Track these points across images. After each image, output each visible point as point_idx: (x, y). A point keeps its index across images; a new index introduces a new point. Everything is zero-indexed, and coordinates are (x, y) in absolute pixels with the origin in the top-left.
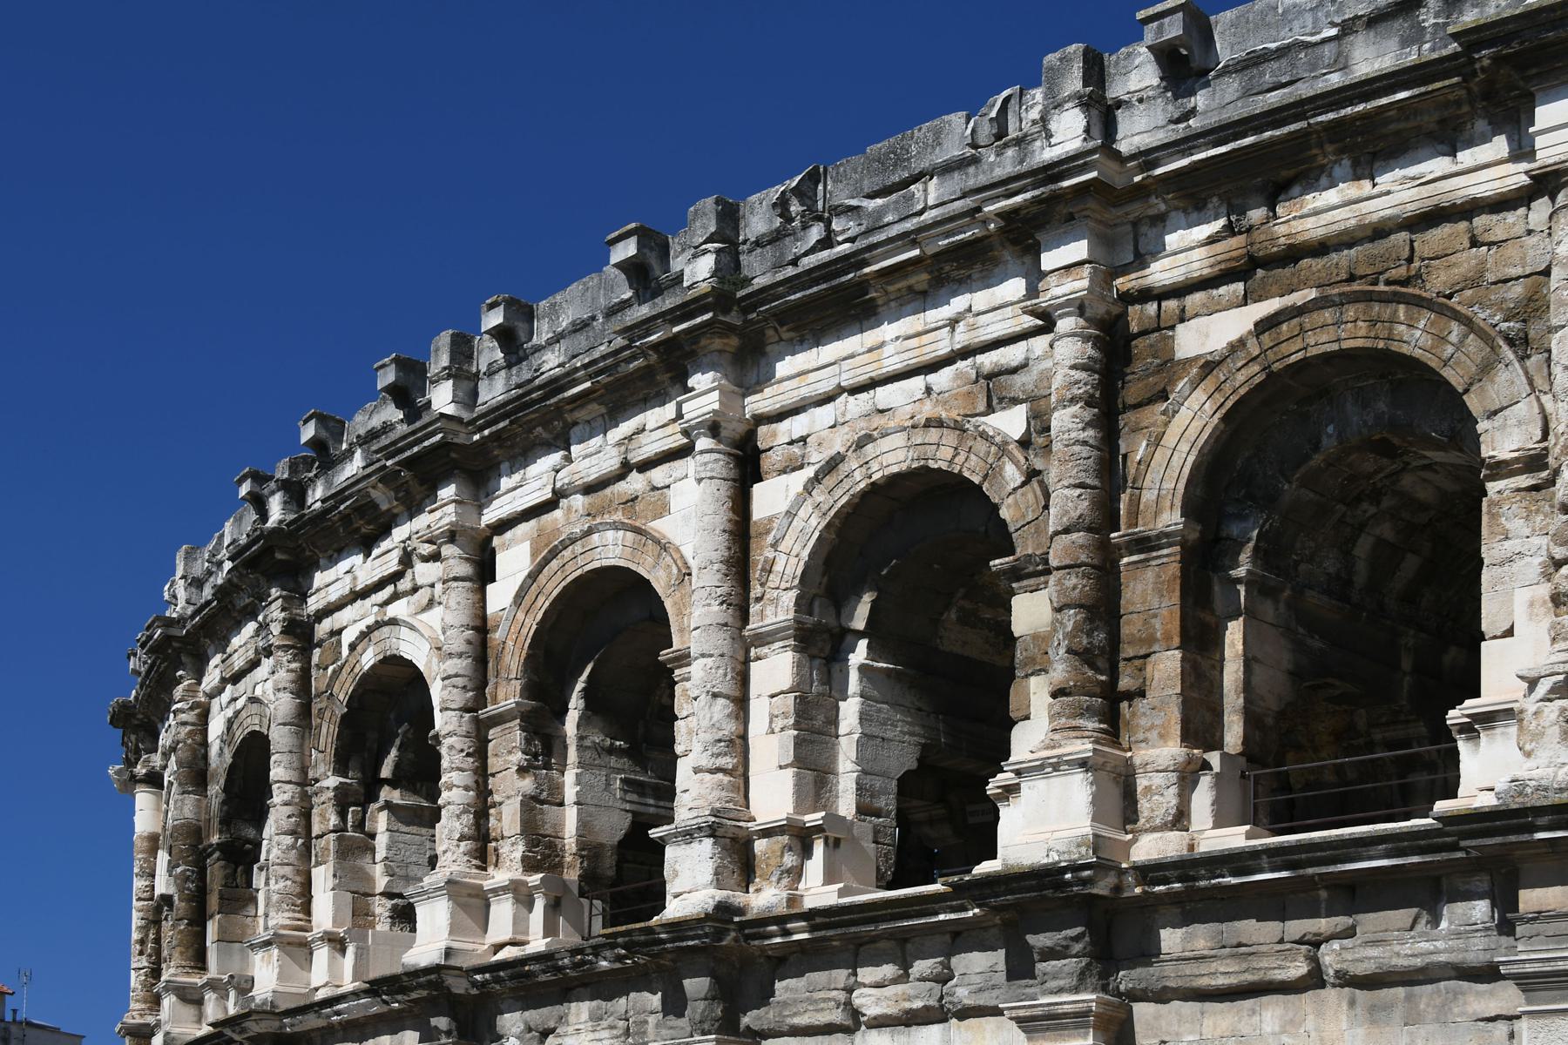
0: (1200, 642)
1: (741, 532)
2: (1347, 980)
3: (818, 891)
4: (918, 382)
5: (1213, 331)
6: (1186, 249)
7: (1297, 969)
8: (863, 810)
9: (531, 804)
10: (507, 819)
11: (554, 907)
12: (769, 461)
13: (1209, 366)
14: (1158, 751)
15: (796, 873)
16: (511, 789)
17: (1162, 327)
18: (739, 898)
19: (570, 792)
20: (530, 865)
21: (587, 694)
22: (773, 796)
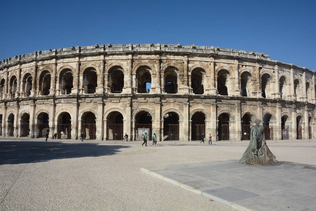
0: (40, 84)
1: (20, 75)
3: (23, 97)
4: (29, 68)
6: (40, 63)
7: (42, 103)
8: (26, 92)
9: (10, 90)
10: (9, 90)
11: (11, 96)
12: (22, 71)
14: (38, 91)
15: (22, 96)
16: (9, 88)
18: (19, 97)
19: (13, 88)
20: (10, 93)
21: (14, 82)
22: (21, 91)
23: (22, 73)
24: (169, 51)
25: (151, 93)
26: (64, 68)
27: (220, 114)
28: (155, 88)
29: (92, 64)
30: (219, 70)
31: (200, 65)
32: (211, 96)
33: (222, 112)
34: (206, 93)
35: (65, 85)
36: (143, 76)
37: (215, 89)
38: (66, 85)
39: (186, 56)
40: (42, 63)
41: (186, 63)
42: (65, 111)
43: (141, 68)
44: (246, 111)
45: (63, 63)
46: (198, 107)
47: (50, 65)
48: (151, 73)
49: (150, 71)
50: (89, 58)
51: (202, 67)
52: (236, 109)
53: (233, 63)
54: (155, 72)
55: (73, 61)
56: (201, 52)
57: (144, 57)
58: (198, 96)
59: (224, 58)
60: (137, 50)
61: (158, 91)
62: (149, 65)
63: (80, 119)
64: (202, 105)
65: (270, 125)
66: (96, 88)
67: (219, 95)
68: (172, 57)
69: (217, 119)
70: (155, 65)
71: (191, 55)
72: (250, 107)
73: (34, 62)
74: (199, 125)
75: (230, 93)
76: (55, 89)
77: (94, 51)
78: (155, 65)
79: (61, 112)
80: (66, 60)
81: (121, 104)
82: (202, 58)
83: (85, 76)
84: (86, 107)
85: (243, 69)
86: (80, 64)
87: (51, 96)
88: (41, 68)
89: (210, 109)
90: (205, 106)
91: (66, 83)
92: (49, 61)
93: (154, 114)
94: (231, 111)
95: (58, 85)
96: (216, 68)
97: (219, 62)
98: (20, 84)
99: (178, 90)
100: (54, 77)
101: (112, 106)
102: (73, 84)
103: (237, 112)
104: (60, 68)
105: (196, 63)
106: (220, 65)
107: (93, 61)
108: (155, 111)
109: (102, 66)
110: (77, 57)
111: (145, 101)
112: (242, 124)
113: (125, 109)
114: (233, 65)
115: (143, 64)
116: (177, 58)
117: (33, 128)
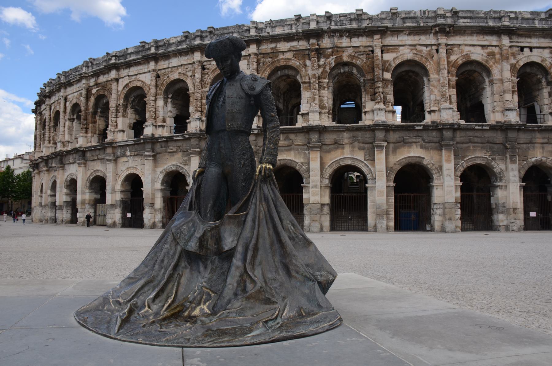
1: (65, 108)
2: (101, 159)
5: (94, 91)
10: (51, 138)
13: (94, 94)
17: (91, 90)
23: (68, 103)
24: (339, 27)
25: (300, 123)
26: (131, 86)
27: (465, 166)
28: (307, 114)
29: (180, 73)
30: (460, 62)
31: (411, 55)
32: (440, 124)
33: (470, 164)
34: (429, 119)
35: (135, 121)
37: (451, 109)
38: (137, 120)
39: (377, 37)
40: (96, 80)
41: (378, 52)
42: (132, 171)
43: (279, 72)
44: (534, 159)
45: (129, 76)
46: (409, 152)
47: (108, 83)
48: (300, 81)
49: (298, 78)
50: (174, 62)
51: (417, 59)
52: (508, 157)
53: (494, 43)
54: (307, 78)
55: (146, 70)
56: (414, 25)
57: (283, 46)
58: (410, 126)
59: (472, 34)
60: (269, 33)
61: (315, 120)
62: (295, 63)
63: (158, 185)
64: (419, 147)
66: (188, 121)
67: (463, 122)
68: (345, 42)
69: (456, 180)
70: (308, 63)
71: (389, 33)
72: (543, 148)
73: (84, 81)
74: (415, 194)
75: (493, 117)
76: (120, 129)
77: (184, 46)
78: (308, 63)
79: (127, 173)
80: (134, 70)
82: (417, 37)
83: (168, 98)
84: (171, 163)
85: (525, 58)
86: (158, 76)
87: (108, 143)
88: (94, 91)
89: (441, 155)
90: (426, 148)
91: (137, 117)
92: (106, 76)
93: (308, 171)
94: (494, 159)
95: (120, 120)
96: (453, 58)
97: (460, 45)
98: (65, 124)
99: (363, 114)
100: (114, 105)
102: (147, 117)
103: (509, 160)
104: (124, 87)
105: (402, 50)
106: (462, 52)
107: (182, 65)
109: (198, 75)
110: (152, 61)
112: (525, 190)
114: (497, 48)
115: (283, 63)
116: (357, 42)
117: (83, 207)
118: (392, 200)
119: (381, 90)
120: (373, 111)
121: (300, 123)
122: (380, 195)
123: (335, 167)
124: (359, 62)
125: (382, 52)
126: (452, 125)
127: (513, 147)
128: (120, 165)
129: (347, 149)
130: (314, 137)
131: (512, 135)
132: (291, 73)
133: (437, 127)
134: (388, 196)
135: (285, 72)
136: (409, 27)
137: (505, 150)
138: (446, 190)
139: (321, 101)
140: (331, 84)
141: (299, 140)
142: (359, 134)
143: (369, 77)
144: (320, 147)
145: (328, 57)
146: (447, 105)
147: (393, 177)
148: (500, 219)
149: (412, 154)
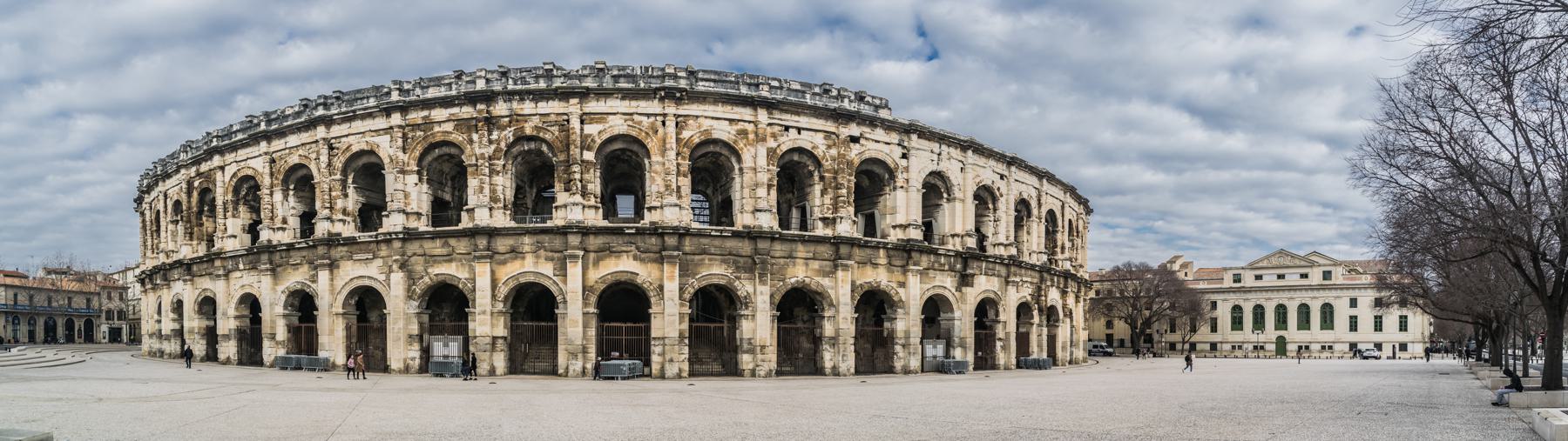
25: (465, 223)
33: (704, 283)
36: (447, 173)
39: (574, 101)
42: (248, 290)
61: (483, 218)
62: (458, 138)
65: (887, 325)
69: (682, 305)
70: (475, 137)
78: (475, 137)
81: (379, 262)
90: (642, 260)
94: (738, 278)
101: (354, 272)
108: (474, 280)
111: (445, 251)
113: (388, 278)
118: (592, 332)
119: (577, 176)
120: (565, 206)
121: (465, 223)
122: (576, 324)
123: (511, 284)
124: (548, 136)
125: (582, 122)
126: (676, 228)
127: (764, 262)
128: (232, 282)
129: (530, 259)
130: (482, 242)
131: (762, 245)
132: (453, 151)
133: (657, 231)
134: (585, 326)
135: (446, 150)
136: (620, 90)
137: (754, 266)
138: (669, 319)
139: (493, 191)
140: (509, 167)
141: (462, 246)
142: (546, 238)
143: (562, 157)
144: (491, 257)
145: (503, 128)
146: (673, 199)
147: (593, 299)
148: (746, 361)
149: (621, 268)
